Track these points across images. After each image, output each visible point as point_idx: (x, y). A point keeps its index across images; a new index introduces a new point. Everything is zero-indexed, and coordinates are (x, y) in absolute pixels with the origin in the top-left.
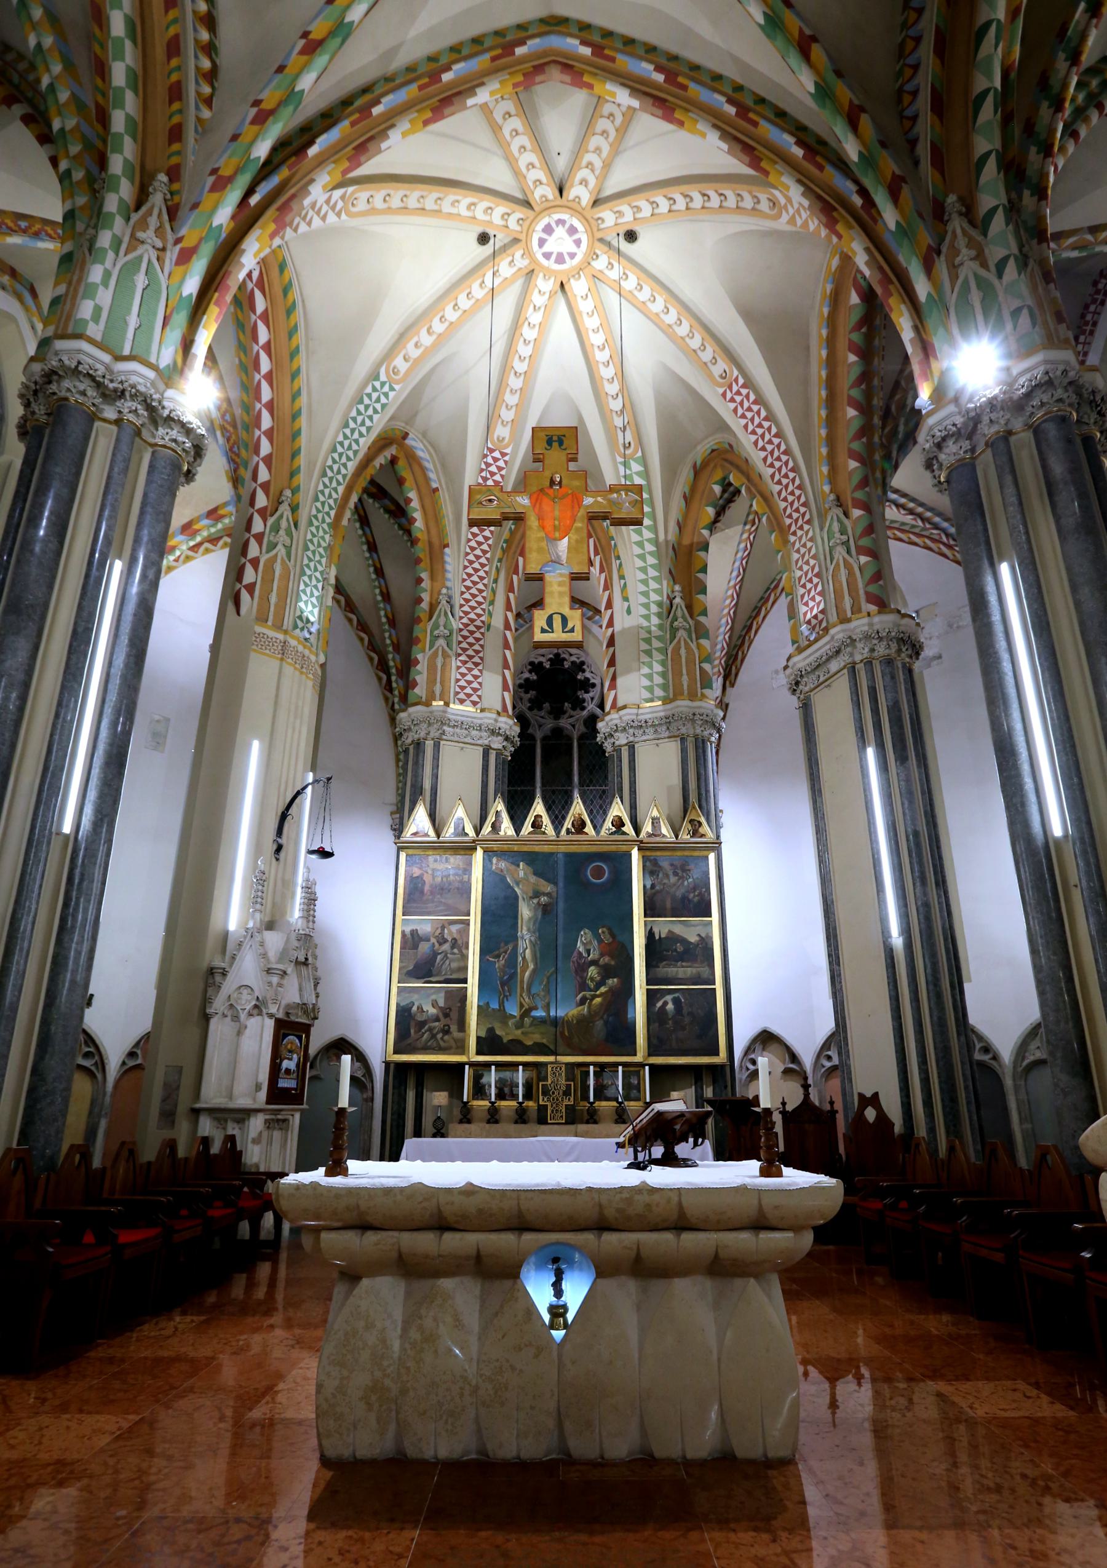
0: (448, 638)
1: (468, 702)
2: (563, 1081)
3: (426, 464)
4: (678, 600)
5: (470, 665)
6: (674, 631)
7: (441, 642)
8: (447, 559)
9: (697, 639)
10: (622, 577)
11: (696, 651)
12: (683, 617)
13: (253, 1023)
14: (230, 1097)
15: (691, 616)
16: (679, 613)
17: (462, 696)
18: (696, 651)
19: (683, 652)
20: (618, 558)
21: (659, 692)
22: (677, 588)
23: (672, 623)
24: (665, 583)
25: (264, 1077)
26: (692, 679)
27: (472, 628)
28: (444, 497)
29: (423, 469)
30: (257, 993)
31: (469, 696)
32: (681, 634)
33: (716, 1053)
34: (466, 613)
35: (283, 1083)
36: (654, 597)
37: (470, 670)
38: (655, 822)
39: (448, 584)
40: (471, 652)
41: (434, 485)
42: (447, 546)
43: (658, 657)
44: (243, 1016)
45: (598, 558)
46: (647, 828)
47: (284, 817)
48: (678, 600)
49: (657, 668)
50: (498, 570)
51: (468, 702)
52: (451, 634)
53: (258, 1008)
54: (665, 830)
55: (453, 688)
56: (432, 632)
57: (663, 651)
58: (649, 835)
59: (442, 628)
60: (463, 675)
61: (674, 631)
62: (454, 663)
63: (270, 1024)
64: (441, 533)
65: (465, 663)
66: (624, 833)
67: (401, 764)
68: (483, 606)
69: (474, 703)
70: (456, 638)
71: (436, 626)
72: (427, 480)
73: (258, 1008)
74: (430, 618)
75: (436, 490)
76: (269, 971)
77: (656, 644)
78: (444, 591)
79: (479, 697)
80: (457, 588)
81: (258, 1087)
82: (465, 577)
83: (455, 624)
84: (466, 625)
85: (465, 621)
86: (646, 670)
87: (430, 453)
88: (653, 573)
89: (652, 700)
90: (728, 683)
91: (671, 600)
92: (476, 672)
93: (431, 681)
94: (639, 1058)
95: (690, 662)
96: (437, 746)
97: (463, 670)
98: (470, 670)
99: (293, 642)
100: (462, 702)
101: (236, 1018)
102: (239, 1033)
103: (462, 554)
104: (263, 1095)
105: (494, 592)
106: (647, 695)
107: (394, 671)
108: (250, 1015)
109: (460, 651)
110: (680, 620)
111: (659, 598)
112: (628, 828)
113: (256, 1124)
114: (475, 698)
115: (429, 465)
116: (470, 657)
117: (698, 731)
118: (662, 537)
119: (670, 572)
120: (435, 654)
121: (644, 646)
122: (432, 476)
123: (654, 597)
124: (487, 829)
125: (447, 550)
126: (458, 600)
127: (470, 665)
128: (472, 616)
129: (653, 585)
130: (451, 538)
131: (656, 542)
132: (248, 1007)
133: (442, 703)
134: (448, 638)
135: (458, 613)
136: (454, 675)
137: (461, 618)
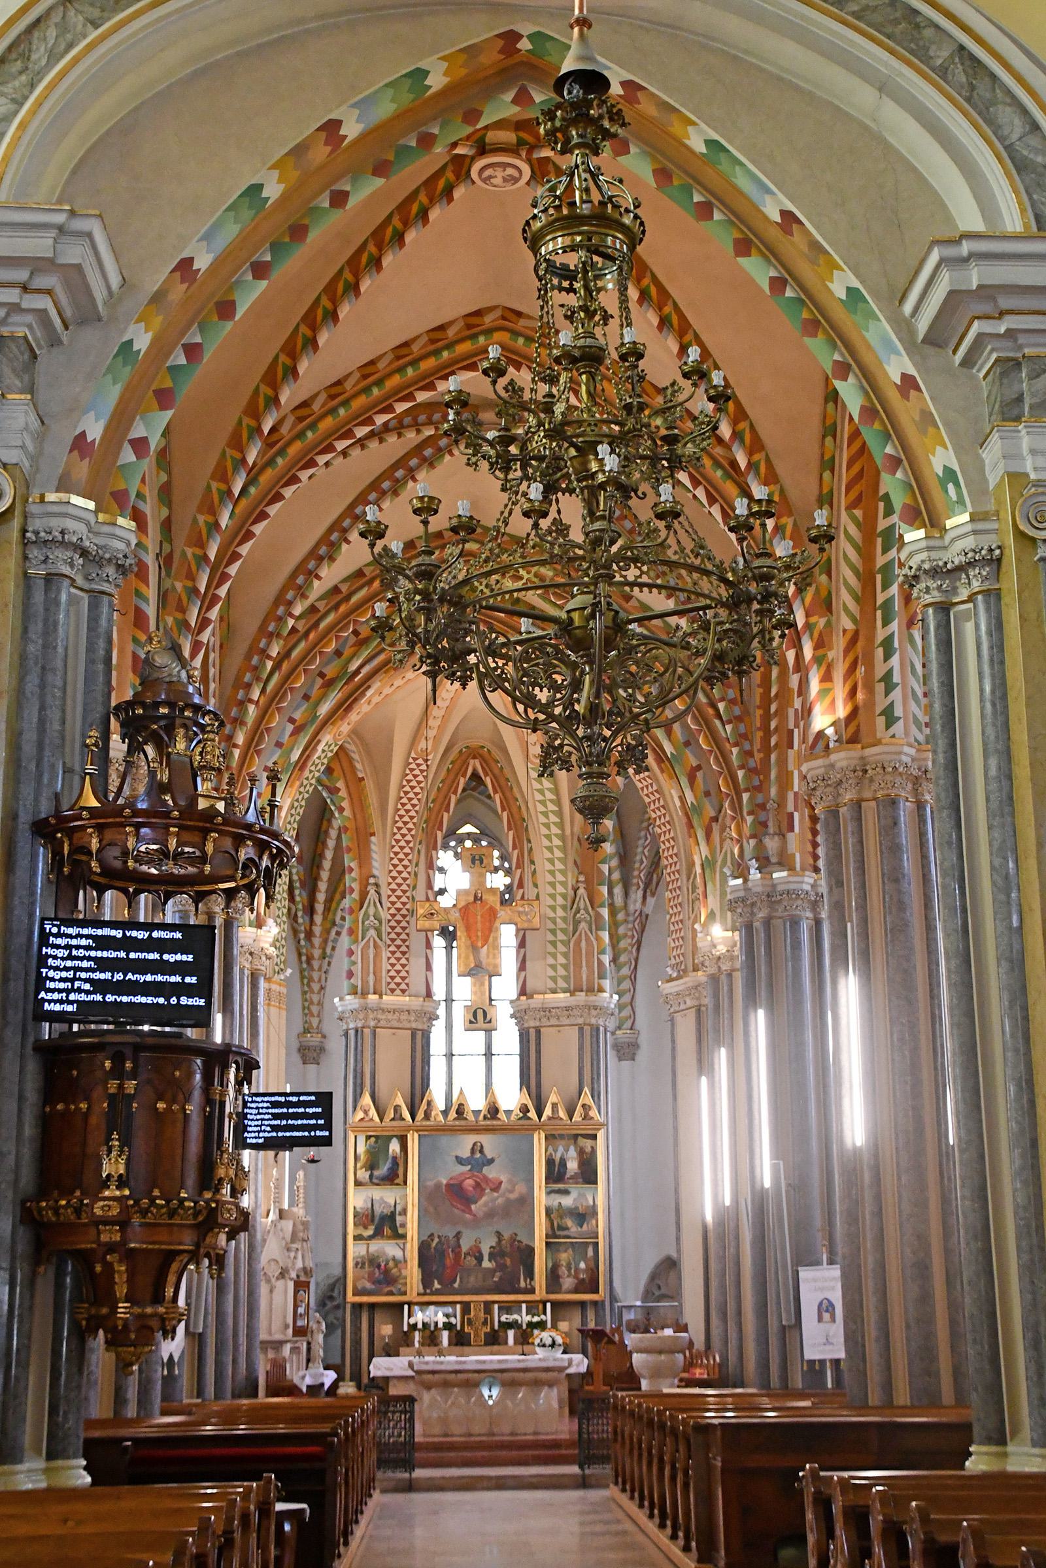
0: (378, 931)
1: (398, 992)
2: (482, 1315)
3: (352, 755)
4: (581, 891)
5: (398, 955)
6: (576, 923)
7: (372, 933)
8: (373, 847)
9: (597, 929)
10: (532, 862)
11: (595, 943)
12: (586, 909)
13: (280, 1284)
14: (270, 1333)
15: (593, 908)
16: (582, 906)
17: (393, 986)
18: (595, 943)
19: (583, 944)
20: (529, 841)
21: (562, 984)
22: (582, 878)
23: (575, 915)
24: (570, 875)
25: (290, 1321)
26: (591, 971)
27: (398, 917)
28: (370, 786)
29: (350, 760)
30: (281, 1264)
31: (398, 984)
32: (583, 926)
33: (596, 1291)
34: (393, 903)
35: (299, 1323)
36: (560, 889)
37: (398, 959)
38: (554, 1106)
39: (376, 872)
40: (398, 942)
41: (360, 775)
42: (373, 834)
43: (561, 948)
44: (273, 1280)
45: (511, 833)
46: (548, 1112)
48: (581, 891)
49: (561, 960)
50: (419, 852)
51: (398, 992)
52: (381, 923)
53: (283, 1274)
54: (562, 1114)
55: (385, 978)
56: (363, 923)
57: (566, 943)
58: (549, 1118)
59: (372, 918)
60: (393, 965)
61: (576, 923)
62: (385, 954)
63: (291, 1285)
64: (367, 820)
65: (393, 953)
66: (529, 1118)
67: (306, 981)
68: (408, 894)
69: (403, 991)
70: (385, 929)
71: (366, 916)
72: (353, 769)
73: (283, 1274)
74: (361, 908)
75: (363, 779)
76: (288, 1250)
77: (561, 936)
78: (372, 880)
79: (407, 984)
80: (383, 880)
81: (287, 1326)
82: (391, 868)
83: (384, 915)
84: (393, 915)
85: (393, 911)
86: (551, 961)
87: (357, 746)
88: (559, 865)
89: (554, 991)
90: (648, 893)
91: (575, 890)
92: (403, 961)
93: (365, 970)
94: (536, 1297)
95: (590, 953)
96: (374, 1034)
97: (393, 961)
98: (398, 959)
99: (274, 987)
100: (393, 991)
101: (268, 1281)
102: (271, 1291)
103: (388, 847)
104: (290, 1331)
105: (416, 875)
106: (551, 985)
107: (298, 885)
108: (278, 1279)
109: (389, 942)
110: (582, 912)
111: (564, 891)
112: (532, 1114)
113: (286, 1350)
114: (403, 986)
115: (356, 756)
116: (398, 947)
117: (593, 1021)
118: (568, 832)
119: (575, 862)
120: (367, 945)
121: (551, 937)
122: (359, 766)
123: (560, 889)
124: (420, 1115)
125: (373, 839)
126: (385, 891)
127: (398, 955)
128: (399, 905)
129: (560, 877)
130: (377, 826)
131: (562, 837)
132: (277, 1274)
133: (377, 997)
134: (378, 931)
135: (386, 904)
136: (385, 966)
137: (389, 909)
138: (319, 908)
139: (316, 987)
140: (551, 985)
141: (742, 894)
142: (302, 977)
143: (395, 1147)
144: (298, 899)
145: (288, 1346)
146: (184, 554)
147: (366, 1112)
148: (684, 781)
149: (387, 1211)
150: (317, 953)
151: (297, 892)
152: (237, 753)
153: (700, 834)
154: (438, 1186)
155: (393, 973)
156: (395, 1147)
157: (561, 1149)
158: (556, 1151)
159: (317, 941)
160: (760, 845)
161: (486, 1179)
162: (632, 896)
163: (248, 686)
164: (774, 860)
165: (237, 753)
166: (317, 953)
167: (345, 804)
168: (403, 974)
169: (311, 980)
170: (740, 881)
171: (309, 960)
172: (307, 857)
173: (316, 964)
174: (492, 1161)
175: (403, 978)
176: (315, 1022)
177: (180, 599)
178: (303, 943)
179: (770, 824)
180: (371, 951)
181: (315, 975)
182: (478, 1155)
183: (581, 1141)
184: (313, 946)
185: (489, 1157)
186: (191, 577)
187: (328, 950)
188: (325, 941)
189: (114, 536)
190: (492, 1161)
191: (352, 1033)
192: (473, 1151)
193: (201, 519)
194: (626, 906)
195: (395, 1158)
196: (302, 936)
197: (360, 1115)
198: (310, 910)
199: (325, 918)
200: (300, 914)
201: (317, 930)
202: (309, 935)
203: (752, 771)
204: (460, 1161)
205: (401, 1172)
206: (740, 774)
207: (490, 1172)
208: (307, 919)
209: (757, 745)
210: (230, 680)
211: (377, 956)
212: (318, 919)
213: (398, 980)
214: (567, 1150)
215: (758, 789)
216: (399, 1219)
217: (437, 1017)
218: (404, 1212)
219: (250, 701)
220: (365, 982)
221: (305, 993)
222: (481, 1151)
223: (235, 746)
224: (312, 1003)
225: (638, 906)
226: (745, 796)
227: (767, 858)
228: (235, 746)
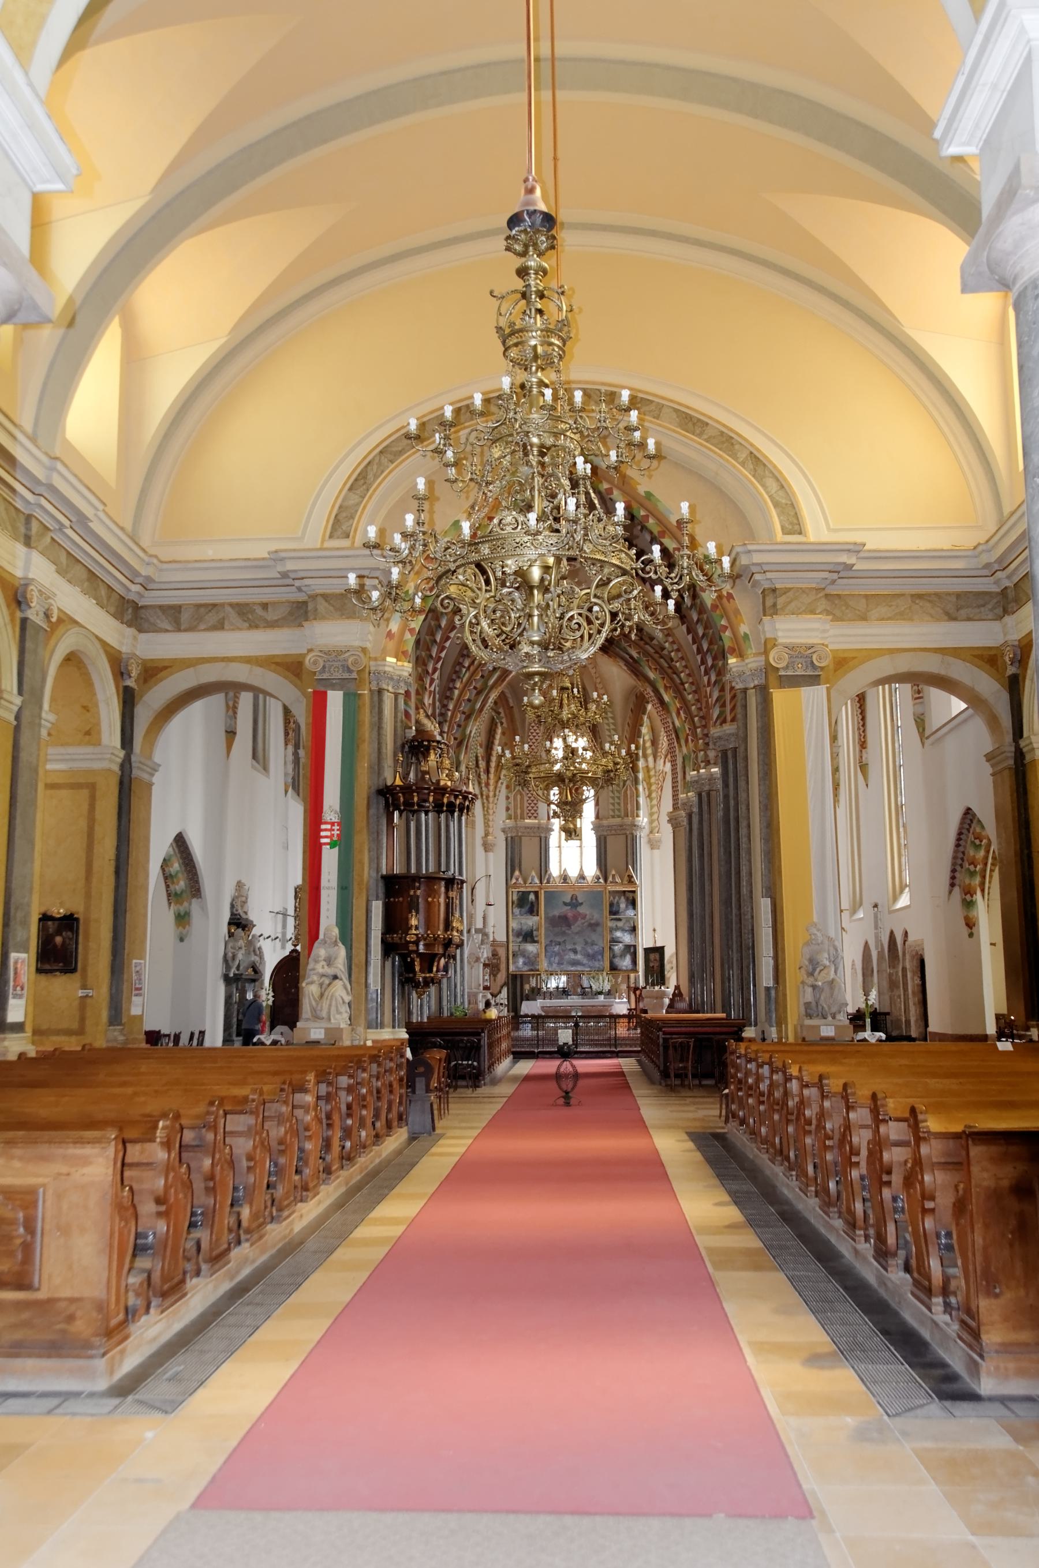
19: (629, 792)
26: (632, 806)
35: (486, 984)
38: (614, 876)
41: (511, 705)
47: (473, 889)
55: (526, 811)
62: (526, 798)
89: (613, 817)
93: (515, 806)
100: (530, 817)
104: (482, 988)
106: (611, 813)
114: (535, 815)
122: (511, 701)
136: (526, 804)
138: (492, 770)
139: (491, 812)
140: (611, 813)
141: (696, 779)
142: (484, 807)
143: (532, 897)
144: (481, 766)
145: (481, 995)
146: (425, 639)
147: (517, 879)
148: (674, 715)
149: (529, 929)
150: (491, 794)
151: (480, 762)
152: (449, 713)
153: (683, 742)
154: (554, 916)
155: (530, 808)
156: (532, 897)
157: (617, 898)
158: (614, 898)
159: (491, 788)
160: (706, 755)
161: (580, 914)
162: (658, 762)
163: (453, 681)
164: (712, 762)
165: (449, 713)
166: (491, 794)
167: (504, 720)
168: (535, 808)
169: (488, 808)
170: (695, 772)
171: (488, 797)
172: (484, 744)
173: (491, 800)
174: (582, 904)
175: (535, 811)
176: (491, 830)
177: (424, 661)
178: (484, 789)
179: (710, 744)
180: (519, 797)
181: (491, 806)
182: (574, 901)
183: (628, 894)
184: (489, 791)
185: (580, 901)
186: (429, 649)
187: (497, 793)
188: (496, 788)
189: (403, 670)
190: (582, 904)
191: (509, 839)
192: (572, 898)
193: (433, 623)
194: (655, 767)
195: (532, 903)
196: (483, 785)
197: (514, 881)
198: (488, 772)
199: (495, 775)
200: (482, 774)
201: (492, 782)
202: (487, 785)
203: (702, 718)
204: (565, 904)
205: (535, 909)
206: (696, 719)
207: (581, 910)
208: (486, 776)
209: (704, 705)
210: (445, 677)
211: (522, 799)
212: (492, 776)
213: (532, 811)
214: (620, 898)
215: (705, 727)
216: (535, 933)
217: (553, 830)
218: (537, 930)
219: (456, 688)
220: (515, 813)
221: (485, 815)
222: (576, 899)
223: (449, 710)
224: (489, 820)
225: (661, 768)
226: (699, 730)
227: (709, 761)
228: (449, 710)
